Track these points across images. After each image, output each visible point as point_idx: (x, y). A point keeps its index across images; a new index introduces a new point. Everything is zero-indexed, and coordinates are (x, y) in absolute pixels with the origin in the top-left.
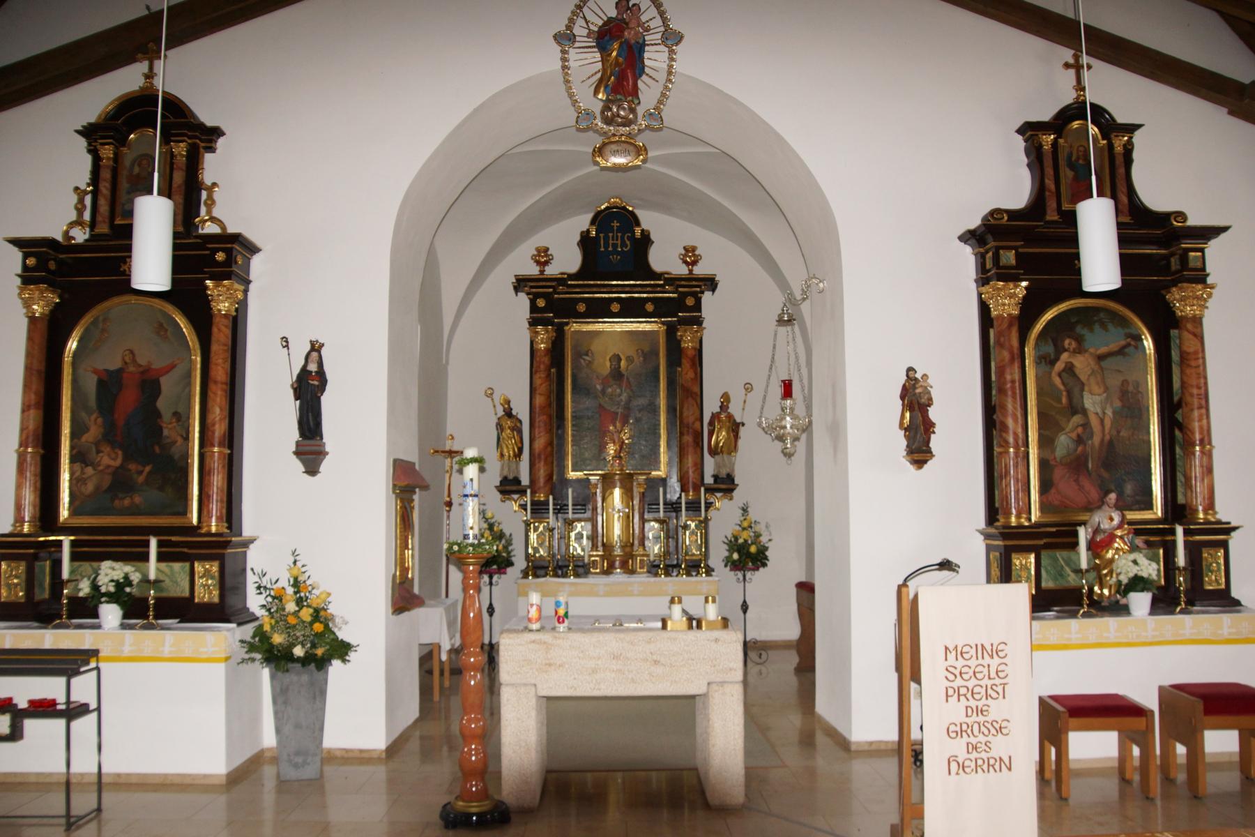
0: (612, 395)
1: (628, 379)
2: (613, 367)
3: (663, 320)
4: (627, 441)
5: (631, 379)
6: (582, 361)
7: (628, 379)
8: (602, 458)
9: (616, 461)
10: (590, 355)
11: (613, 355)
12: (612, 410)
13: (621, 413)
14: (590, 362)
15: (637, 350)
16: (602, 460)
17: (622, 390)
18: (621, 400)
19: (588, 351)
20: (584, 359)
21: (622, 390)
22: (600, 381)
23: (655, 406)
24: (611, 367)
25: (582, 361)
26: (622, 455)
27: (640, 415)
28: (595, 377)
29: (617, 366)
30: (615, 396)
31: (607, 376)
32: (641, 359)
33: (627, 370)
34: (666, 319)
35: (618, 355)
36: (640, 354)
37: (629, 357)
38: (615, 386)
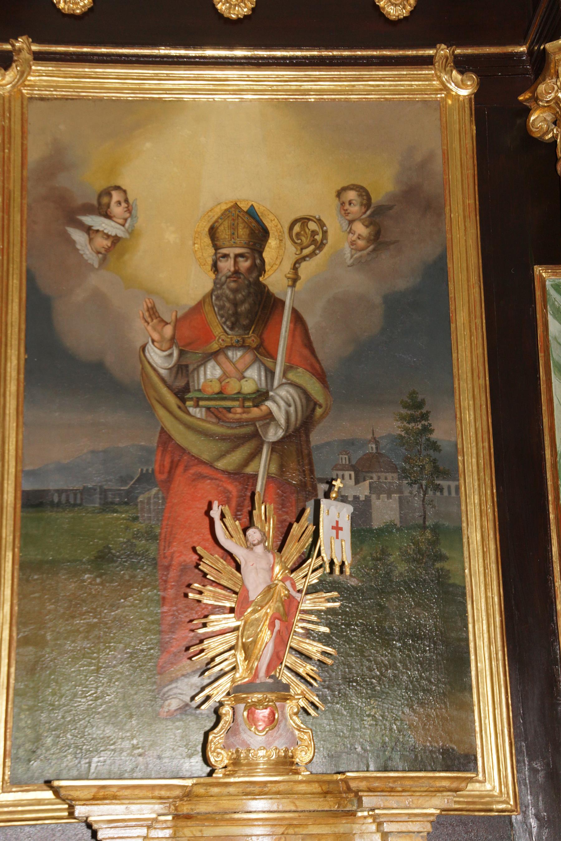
0: (221, 395)
1: (297, 317)
2: (227, 266)
3: (458, 51)
4: (307, 604)
5: (311, 321)
6: (78, 236)
7: (297, 317)
8: (174, 704)
9: (251, 708)
10: (117, 210)
11: (226, 214)
12: (220, 465)
13: (269, 478)
14: (116, 240)
15: (339, 194)
16: (171, 716)
17: (270, 373)
18: (270, 417)
19: (107, 193)
20: (88, 230)
21: (270, 373)
22: (168, 331)
23: (434, 446)
24: (215, 267)
25: (78, 236)
26: (286, 677)
27: (363, 490)
28: (141, 309)
29: (244, 264)
30: (242, 398)
31: (199, 306)
32: (360, 228)
33: (295, 280)
34: (469, 51)
35: (252, 213)
36: (355, 209)
37: (304, 221)
38: (236, 355)
